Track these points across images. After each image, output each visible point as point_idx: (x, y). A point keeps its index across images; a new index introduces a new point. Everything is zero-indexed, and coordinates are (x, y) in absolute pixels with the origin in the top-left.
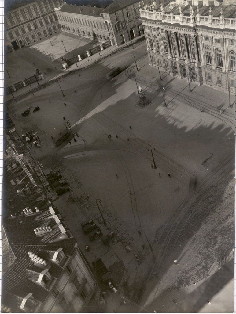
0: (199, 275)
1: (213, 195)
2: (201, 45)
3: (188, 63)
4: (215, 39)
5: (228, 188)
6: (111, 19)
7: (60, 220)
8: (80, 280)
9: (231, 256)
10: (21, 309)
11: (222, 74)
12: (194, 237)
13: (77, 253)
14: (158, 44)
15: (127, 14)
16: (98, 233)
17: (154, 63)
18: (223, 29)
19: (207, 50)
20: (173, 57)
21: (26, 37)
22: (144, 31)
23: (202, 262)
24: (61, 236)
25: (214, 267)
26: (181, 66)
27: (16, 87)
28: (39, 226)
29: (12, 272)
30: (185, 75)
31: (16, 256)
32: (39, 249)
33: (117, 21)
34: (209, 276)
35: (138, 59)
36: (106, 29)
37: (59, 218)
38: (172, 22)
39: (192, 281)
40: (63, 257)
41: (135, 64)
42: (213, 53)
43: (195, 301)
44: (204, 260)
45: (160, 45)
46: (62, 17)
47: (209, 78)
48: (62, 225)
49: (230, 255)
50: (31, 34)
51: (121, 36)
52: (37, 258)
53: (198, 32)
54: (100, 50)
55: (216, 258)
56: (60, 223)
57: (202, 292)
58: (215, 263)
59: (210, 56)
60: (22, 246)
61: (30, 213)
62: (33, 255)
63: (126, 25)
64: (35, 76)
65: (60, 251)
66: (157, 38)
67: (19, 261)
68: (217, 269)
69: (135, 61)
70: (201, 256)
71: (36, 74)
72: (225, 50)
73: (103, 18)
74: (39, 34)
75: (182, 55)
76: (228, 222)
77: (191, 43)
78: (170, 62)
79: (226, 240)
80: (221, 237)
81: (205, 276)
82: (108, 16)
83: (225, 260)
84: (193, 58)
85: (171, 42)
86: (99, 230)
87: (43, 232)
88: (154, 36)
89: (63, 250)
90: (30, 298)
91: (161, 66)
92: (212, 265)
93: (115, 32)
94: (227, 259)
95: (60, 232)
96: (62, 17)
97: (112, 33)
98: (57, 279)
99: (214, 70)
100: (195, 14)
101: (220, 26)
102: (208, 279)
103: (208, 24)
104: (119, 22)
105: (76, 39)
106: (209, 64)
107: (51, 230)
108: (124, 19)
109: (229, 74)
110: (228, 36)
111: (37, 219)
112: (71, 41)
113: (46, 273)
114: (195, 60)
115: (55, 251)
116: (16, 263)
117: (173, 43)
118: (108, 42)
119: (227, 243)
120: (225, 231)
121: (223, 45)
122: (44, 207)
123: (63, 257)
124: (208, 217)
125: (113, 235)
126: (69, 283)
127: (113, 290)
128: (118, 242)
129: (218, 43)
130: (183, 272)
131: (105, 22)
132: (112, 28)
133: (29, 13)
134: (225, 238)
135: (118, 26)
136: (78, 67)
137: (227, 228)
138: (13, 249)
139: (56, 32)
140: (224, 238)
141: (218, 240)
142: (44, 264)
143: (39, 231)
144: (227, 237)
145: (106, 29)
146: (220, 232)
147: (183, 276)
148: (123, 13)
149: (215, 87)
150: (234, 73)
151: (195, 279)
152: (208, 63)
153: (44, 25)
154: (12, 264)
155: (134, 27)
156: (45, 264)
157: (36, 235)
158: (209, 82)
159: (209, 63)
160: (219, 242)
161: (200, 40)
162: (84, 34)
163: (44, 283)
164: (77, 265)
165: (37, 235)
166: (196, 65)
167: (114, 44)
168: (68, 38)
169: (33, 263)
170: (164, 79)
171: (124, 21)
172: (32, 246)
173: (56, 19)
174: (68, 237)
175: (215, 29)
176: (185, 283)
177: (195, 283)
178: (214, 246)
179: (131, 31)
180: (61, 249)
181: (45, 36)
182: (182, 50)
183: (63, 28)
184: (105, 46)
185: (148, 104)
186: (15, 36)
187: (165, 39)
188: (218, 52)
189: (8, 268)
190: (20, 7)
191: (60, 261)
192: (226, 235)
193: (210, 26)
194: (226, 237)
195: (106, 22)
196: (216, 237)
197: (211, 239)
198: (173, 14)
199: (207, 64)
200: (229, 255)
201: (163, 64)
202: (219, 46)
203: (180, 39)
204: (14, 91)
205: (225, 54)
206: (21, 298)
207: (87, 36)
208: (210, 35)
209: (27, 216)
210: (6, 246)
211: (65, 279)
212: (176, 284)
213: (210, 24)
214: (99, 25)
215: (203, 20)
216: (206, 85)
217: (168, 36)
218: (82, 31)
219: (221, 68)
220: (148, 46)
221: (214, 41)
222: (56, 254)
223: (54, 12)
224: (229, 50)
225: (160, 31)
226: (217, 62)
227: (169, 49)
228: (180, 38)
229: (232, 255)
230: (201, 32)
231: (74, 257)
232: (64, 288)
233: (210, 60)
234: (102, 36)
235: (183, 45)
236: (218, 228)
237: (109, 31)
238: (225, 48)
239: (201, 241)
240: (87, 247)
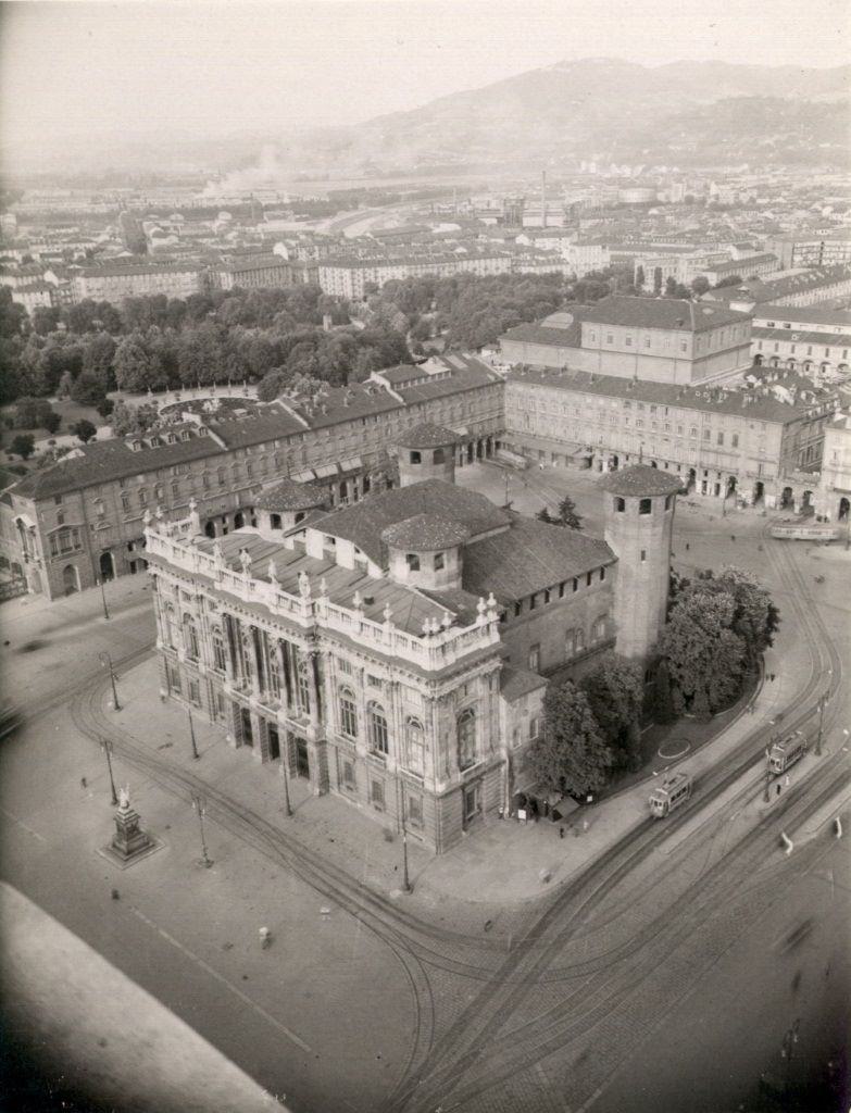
2: (328, 682)
4: (371, 677)
18: (391, 657)
19: (345, 697)
20: (239, 690)
42: (360, 710)
47: (348, 775)
59: (353, 715)
66: (193, 619)
72: (395, 709)
73: (12, 506)
77: (298, 664)
78: (228, 704)
84: (301, 706)
85: (237, 646)
88: (185, 614)
99: (363, 759)
100: (315, 594)
106: (350, 736)
114: (308, 712)
117: (245, 648)
152: (345, 733)
158: (348, 788)
159: (349, 732)
175: (370, 651)
182: (269, 675)
185: (148, 849)
188: (378, 713)
198: (250, 575)
199: (343, 736)
201: (205, 701)
205: (396, 726)
208: (357, 662)
215: (338, 617)
216: (337, 795)
220: (160, 637)
221: (365, 679)
224: (406, 714)
225: (206, 605)
227: (229, 664)
228: (266, 643)
233: (353, 725)
235: (272, 662)
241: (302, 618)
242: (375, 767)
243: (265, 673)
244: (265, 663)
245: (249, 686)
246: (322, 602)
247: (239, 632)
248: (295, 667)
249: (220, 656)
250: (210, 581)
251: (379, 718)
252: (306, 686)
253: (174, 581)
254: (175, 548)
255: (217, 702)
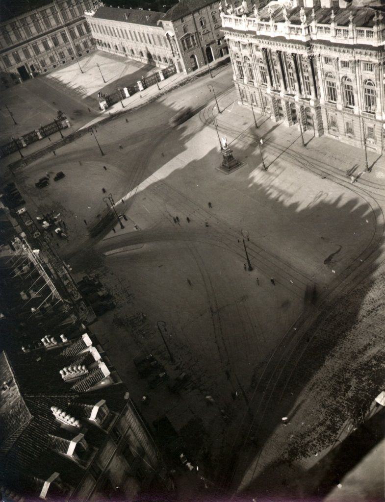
0: (323, 441)
1: (342, 313)
3: (299, 101)
5: (366, 301)
6: (175, 30)
7: (100, 354)
8: (133, 450)
9: (372, 410)
10: (43, 498)
11: (354, 118)
12: (314, 380)
13: (129, 408)
14: (251, 70)
15: (201, 22)
16: (161, 375)
17: (245, 101)
18: (354, 45)
20: (274, 91)
21: (40, 59)
22: (229, 50)
23: (326, 420)
24: (103, 381)
25: (346, 426)
26: (288, 105)
27: (25, 141)
28: (67, 366)
29: (26, 440)
30: (294, 119)
31: (32, 414)
32: (69, 402)
33: (185, 33)
34: (338, 443)
35: (220, 94)
36: (167, 46)
37: (99, 351)
38: (272, 33)
39: (311, 449)
40: (107, 414)
41: (215, 102)
42: (338, 84)
43: (316, 483)
44: (330, 416)
45: (253, 71)
46: (97, 27)
47: (334, 124)
48: (103, 363)
49: (371, 408)
50: (49, 55)
51: (193, 56)
52: (66, 416)
53: (314, 50)
54: (159, 81)
55: (349, 414)
56: (101, 360)
57: (328, 467)
58: (347, 421)
59: (334, 89)
60: (41, 397)
61: (53, 345)
62: (59, 412)
63: (199, 40)
64: (56, 122)
65: (103, 404)
66: (249, 59)
67: (37, 421)
68: (351, 430)
69: (215, 97)
70: (326, 410)
71: (57, 119)
73: (163, 28)
74: (62, 55)
75: (290, 87)
76: (368, 355)
77: (303, 68)
78: (270, 99)
79: (364, 384)
80: (356, 379)
81: (332, 442)
82: (170, 24)
83: (364, 415)
85: (271, 66)
86: (163, 370)
87: (73, 374)
88: (245, 57)
89: (106, 403)
90: (56, 480)
91: (257, 106)
92: (342, 425)
93: (183, 50)
94: (366, 414)
95: (101, 374)
96: (97, 27)
97: (177, 53)
98: (98, 449)
99: (340, 111)
100: (309, 21)
101: (350, 40)
102: (338, 446)
103: (329, 37)
104: (188, 35)
105: (121, 63)
106: (333, 101)
107: (87, 372)
108: (197, 29)
109: (365, 117)
110: (362, 56)
111: (63, 354)
112: (112, 65)
113: (81, 441)
114: (311, 94)
115: (94, 404)
116: (33, 425)
117: (275, 68)
118: (172, 66)
119: (366, 388)
120: (362, 370)
121: (354, 72)
122: (75, 336)
123: (107, 414)
124: (336, 347)
125: (186, 379)
126: (117, 456)
127: (187, 466)
128: (193, 389)
129: (346, 68)
130: (298, 436)
131: (165, 35)
132: (177, 45)
133: (44, 21)
134: (362, 382)
135: (187, 41)
136: (123, 107)
137: (365, 365)
138: (26, 403)
139: (88, 52)
140: (361, 381)
141: (351, 384)
142: (76, 426)
143: (67, 373)
144: (366, 379)
145: (167, 46)
146: (354, 372)
147: (297, 442)
148: (194, 19)
149: (343, 139)
150: (372, 116)
151: (315, 447)
153: (69, 40)
154: (26, 426)
155: (212, 43)
156: (78, 426)
157: (63, 379)
158: (334, 130)
159: (332, 99)
160: (353, 388)
161: (318, 63)
162: (133, 55)
163: (77, 457)
164: (130, 427)
165: (65, 380)
166: (312, 103)
167: (181, 70)
168: (109, 60)
169: (59, 424)
170: (261, 127)
171: (197, 32)
172: (57, 398)
173: (88, 30)
174: (113, 382)
175: (341, 45)
176: (300, 454)
177: (316, 454)
178: (345, 394)
179: (208, 50)
180: (103, 402)
181: (70, 58)
182: (289, 79)
183: (100, 45)
184: (167, 73)
185: (238, 166)
186: (22, 57)
187: (261, 62)
188: (347, 83)
189: (20, 433)
190: (30, 11)
191: (103, 421)
192: (364, 376)
193: (333, 41)
194: (364, 379)
195: (167, 35)
196: (349, 380)
197: (341, 382)
198: (274, 21)
199: (329, 102)
200: (369, 408)
201: (259, 102)
202: (347, 72)
203: (286, 61)
204: (23, 147)
205: (358, 85)
206: (41, 481)
207: (138, 58)
208: (333, 54)
209: (48, 349)
210: (15, 398)
211: (110, 449)
212: (286, 456)
213: (332, 37)
214: (157, 40)
215: (322, 31)
217: (267, 57)
218: (130, 49)
219: (352, 109)
220: (234, 74)
222: (95, 410)
223: (85, 18)
224: (364, 79)
226: (345, 98)
227: (268, 78)
228: (286, 61)
229: (374, 408)
230: (319, 50)
231: (124, 414)
232: (109, 464)
233: (334, 95)
234: (162, 58)
235: (290, 71)
236: (351, 364)
237: (172, 50)
238: (357, 76)
239: (325, 386)
240: (144, 397)
241: (302, 37)
242: (348, 114)
243: (287, 78)
244: (286, 72)
245: (279, 88)
246: (313, 24)
247: (271, 59)
248: (302, 73)
249: (263, 75)
250: (254, 33)
251: (348, 86)
252: (308, 80)
253: (237, 39)
254: (236, 20)
255: (265, 101)
